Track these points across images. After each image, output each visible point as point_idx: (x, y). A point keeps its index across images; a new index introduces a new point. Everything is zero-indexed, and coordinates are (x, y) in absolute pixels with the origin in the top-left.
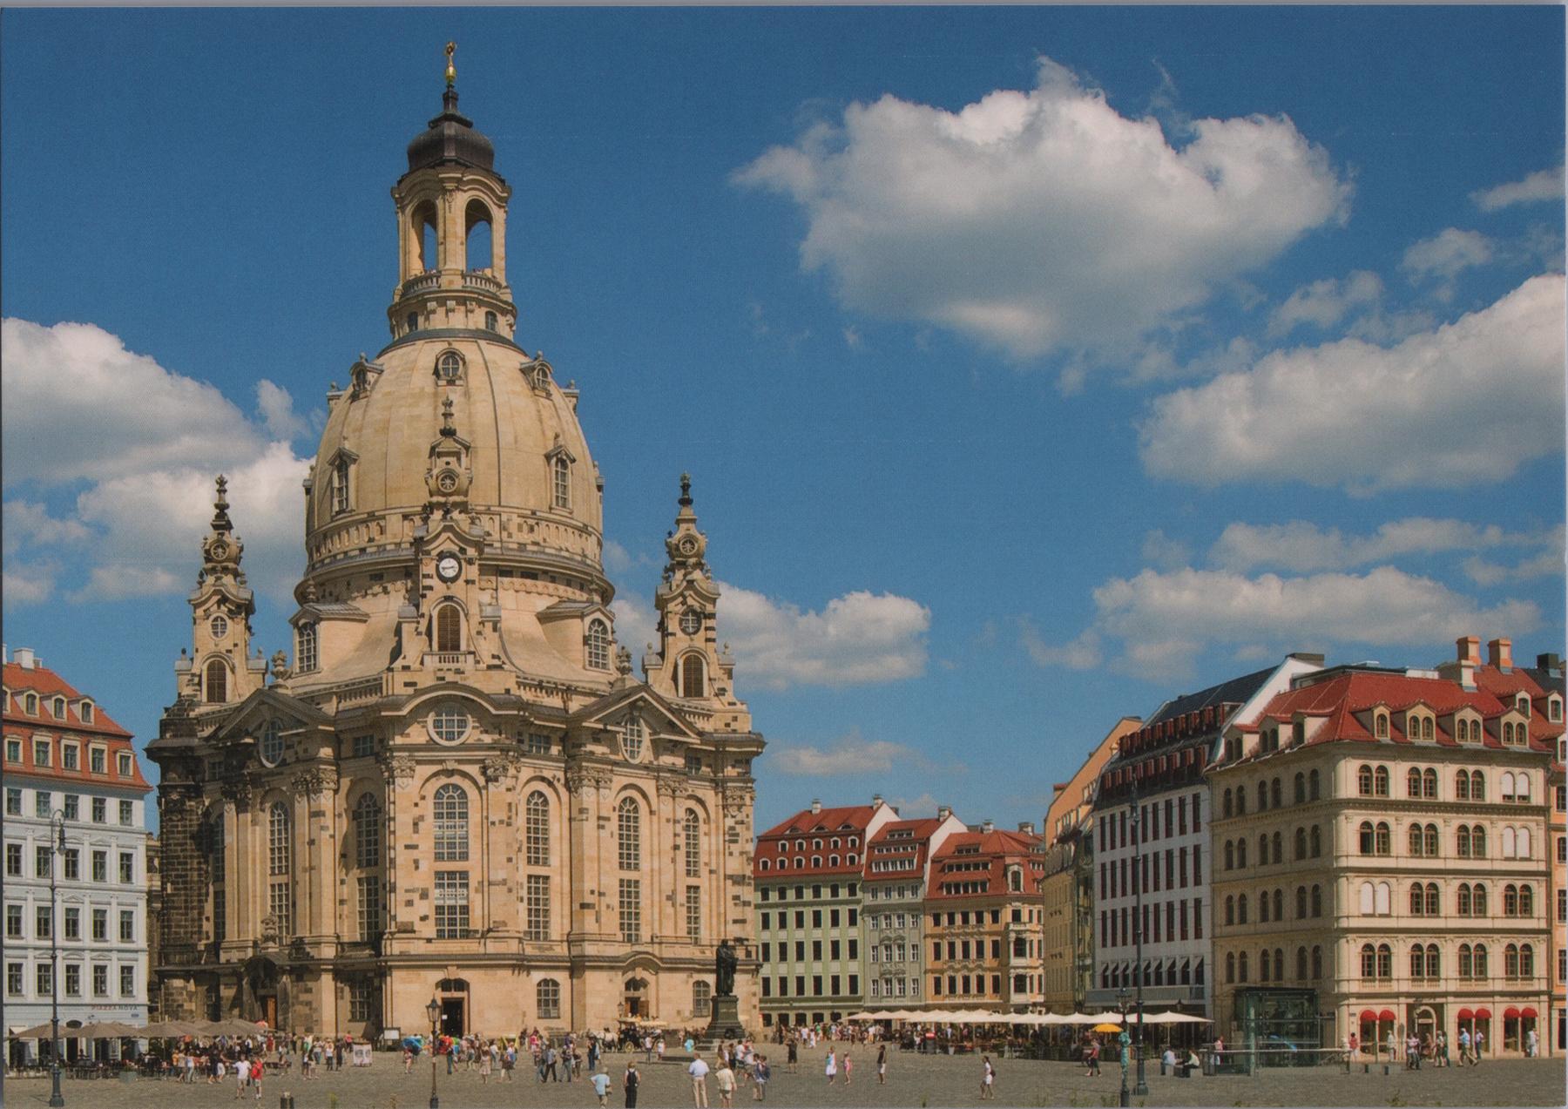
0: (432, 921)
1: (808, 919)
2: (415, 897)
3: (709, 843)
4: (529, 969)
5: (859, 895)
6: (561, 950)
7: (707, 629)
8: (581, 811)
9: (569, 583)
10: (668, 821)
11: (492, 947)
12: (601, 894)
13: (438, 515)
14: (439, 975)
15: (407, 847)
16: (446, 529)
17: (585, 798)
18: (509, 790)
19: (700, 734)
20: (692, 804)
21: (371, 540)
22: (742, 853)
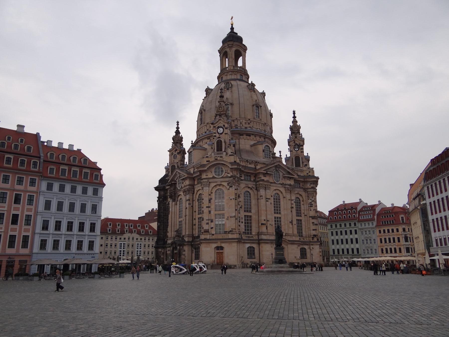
0: (214, 229)
3: (304, 207)
4: (244, 243)
5: (357, 226)
6: (256, 238)
7: (301, 149)
8: (261, 196)
12: (268, 221)
13: (218, 117)
14: (215, 245)
15: (207, 207)
17: (261, 192)
19: (298, 175)
20: (298, 196)
21: (208, 130)
22: (314, 210)
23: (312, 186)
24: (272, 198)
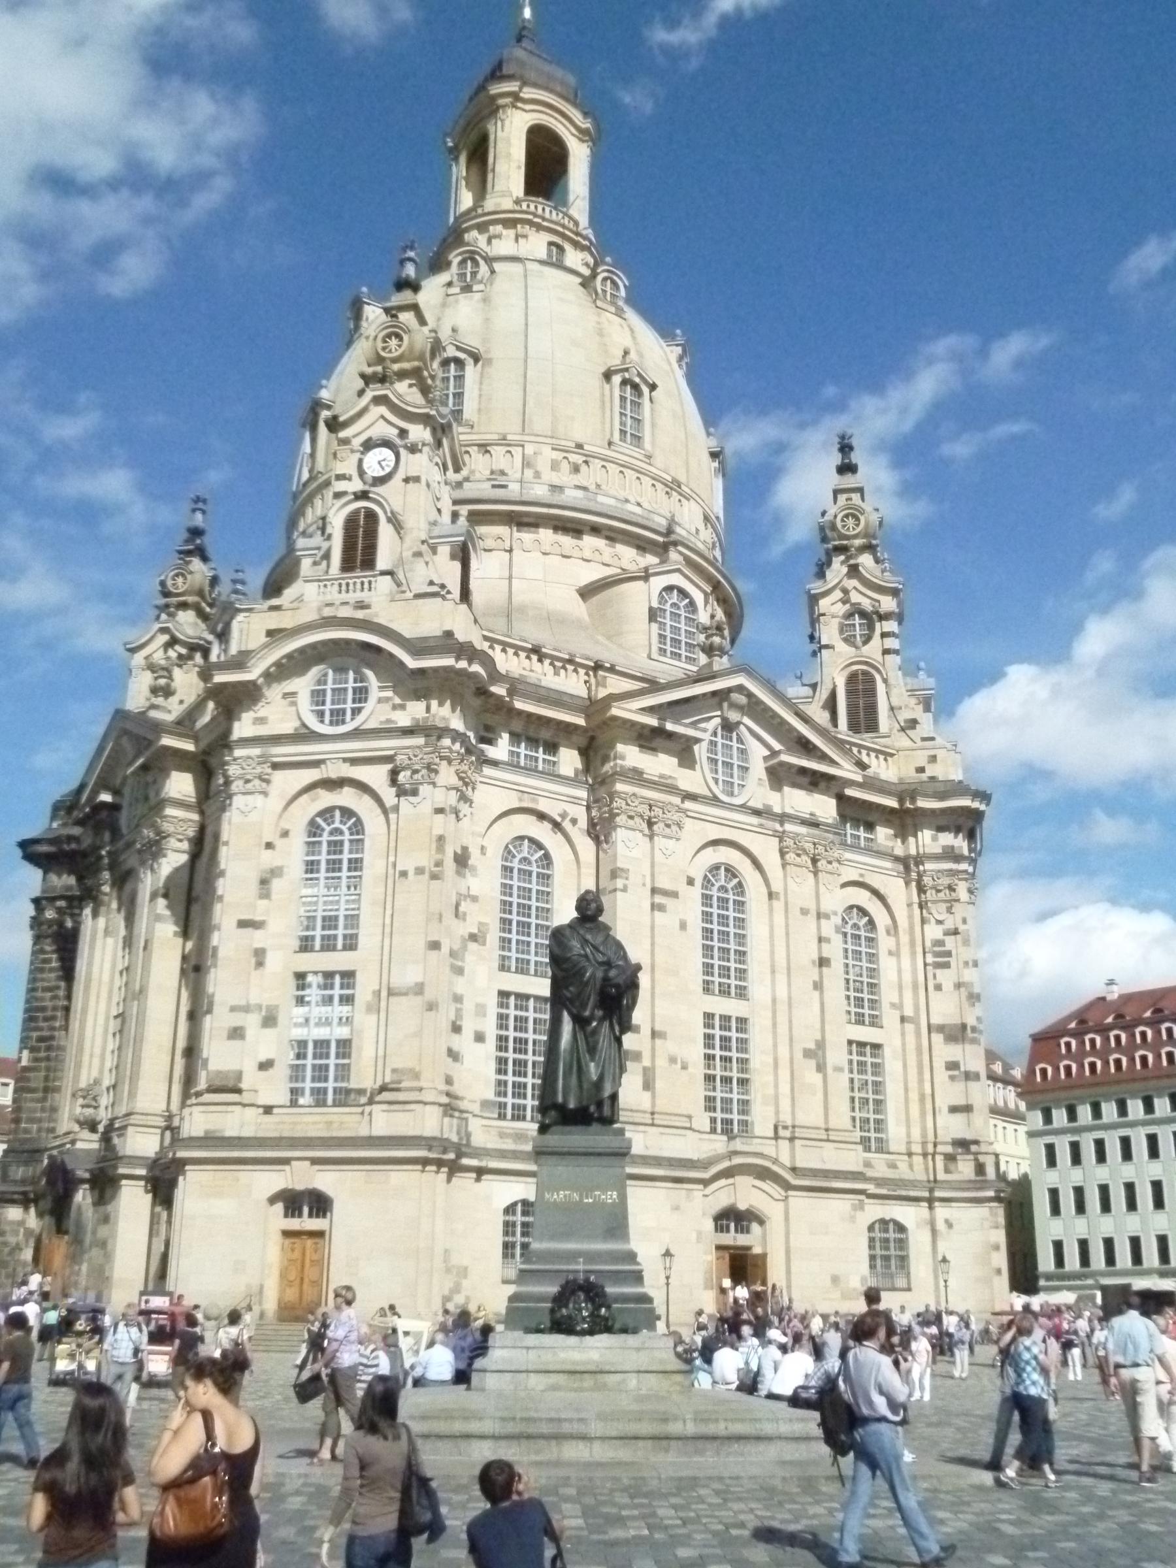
0: (281, 1072)
1: (1113, 1149)
2: (252, 1022)
3: (896, 970)
7: (884, 635)
8: (614, 874)
9: (643, 545)
10: (804, 912)
11: (383, 1122)
15: (243, 924)
16: (379, 400)
17: (620, 847)
18: (440, 811)
19: (862, 766)
20: (863, 898)
22: (958, 986)
23: (948, 839)
24: (697, 891)
